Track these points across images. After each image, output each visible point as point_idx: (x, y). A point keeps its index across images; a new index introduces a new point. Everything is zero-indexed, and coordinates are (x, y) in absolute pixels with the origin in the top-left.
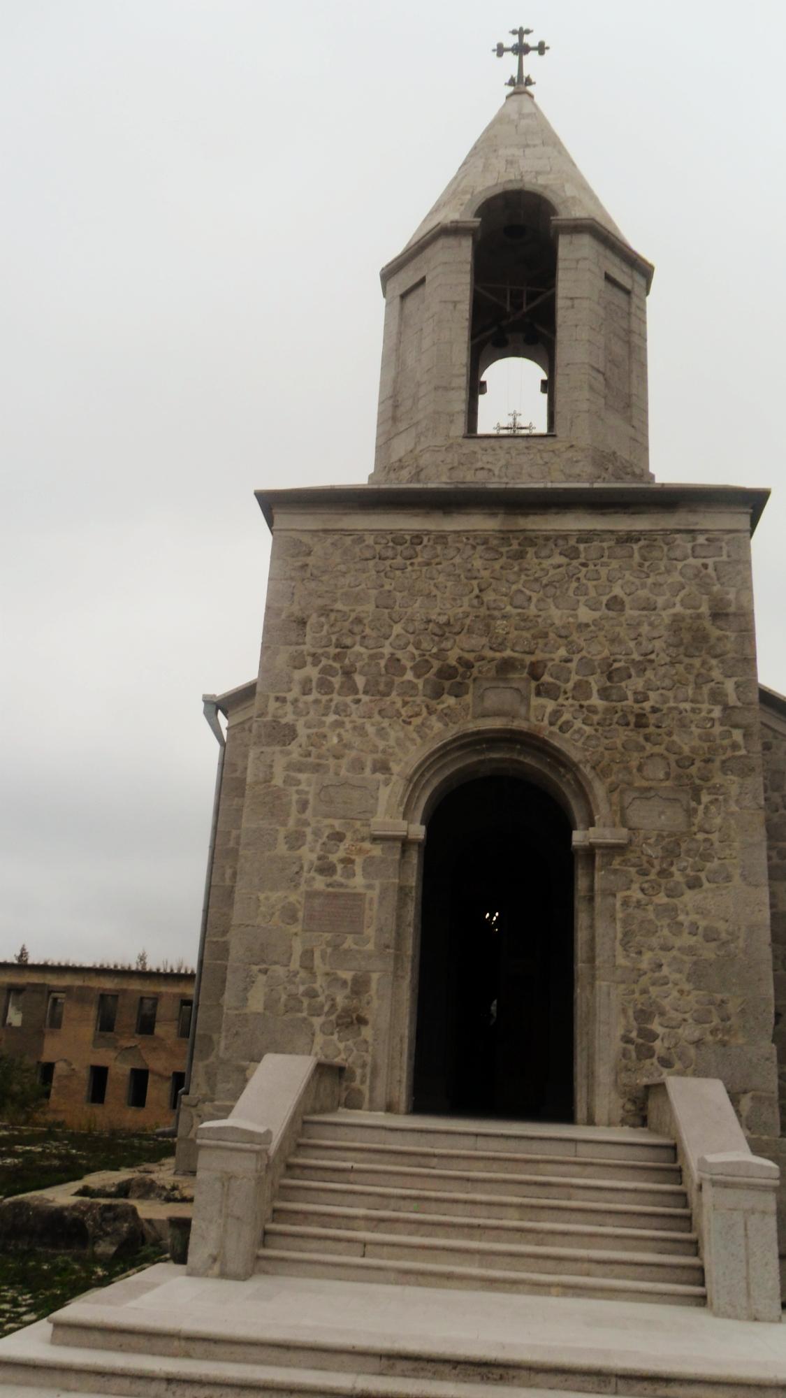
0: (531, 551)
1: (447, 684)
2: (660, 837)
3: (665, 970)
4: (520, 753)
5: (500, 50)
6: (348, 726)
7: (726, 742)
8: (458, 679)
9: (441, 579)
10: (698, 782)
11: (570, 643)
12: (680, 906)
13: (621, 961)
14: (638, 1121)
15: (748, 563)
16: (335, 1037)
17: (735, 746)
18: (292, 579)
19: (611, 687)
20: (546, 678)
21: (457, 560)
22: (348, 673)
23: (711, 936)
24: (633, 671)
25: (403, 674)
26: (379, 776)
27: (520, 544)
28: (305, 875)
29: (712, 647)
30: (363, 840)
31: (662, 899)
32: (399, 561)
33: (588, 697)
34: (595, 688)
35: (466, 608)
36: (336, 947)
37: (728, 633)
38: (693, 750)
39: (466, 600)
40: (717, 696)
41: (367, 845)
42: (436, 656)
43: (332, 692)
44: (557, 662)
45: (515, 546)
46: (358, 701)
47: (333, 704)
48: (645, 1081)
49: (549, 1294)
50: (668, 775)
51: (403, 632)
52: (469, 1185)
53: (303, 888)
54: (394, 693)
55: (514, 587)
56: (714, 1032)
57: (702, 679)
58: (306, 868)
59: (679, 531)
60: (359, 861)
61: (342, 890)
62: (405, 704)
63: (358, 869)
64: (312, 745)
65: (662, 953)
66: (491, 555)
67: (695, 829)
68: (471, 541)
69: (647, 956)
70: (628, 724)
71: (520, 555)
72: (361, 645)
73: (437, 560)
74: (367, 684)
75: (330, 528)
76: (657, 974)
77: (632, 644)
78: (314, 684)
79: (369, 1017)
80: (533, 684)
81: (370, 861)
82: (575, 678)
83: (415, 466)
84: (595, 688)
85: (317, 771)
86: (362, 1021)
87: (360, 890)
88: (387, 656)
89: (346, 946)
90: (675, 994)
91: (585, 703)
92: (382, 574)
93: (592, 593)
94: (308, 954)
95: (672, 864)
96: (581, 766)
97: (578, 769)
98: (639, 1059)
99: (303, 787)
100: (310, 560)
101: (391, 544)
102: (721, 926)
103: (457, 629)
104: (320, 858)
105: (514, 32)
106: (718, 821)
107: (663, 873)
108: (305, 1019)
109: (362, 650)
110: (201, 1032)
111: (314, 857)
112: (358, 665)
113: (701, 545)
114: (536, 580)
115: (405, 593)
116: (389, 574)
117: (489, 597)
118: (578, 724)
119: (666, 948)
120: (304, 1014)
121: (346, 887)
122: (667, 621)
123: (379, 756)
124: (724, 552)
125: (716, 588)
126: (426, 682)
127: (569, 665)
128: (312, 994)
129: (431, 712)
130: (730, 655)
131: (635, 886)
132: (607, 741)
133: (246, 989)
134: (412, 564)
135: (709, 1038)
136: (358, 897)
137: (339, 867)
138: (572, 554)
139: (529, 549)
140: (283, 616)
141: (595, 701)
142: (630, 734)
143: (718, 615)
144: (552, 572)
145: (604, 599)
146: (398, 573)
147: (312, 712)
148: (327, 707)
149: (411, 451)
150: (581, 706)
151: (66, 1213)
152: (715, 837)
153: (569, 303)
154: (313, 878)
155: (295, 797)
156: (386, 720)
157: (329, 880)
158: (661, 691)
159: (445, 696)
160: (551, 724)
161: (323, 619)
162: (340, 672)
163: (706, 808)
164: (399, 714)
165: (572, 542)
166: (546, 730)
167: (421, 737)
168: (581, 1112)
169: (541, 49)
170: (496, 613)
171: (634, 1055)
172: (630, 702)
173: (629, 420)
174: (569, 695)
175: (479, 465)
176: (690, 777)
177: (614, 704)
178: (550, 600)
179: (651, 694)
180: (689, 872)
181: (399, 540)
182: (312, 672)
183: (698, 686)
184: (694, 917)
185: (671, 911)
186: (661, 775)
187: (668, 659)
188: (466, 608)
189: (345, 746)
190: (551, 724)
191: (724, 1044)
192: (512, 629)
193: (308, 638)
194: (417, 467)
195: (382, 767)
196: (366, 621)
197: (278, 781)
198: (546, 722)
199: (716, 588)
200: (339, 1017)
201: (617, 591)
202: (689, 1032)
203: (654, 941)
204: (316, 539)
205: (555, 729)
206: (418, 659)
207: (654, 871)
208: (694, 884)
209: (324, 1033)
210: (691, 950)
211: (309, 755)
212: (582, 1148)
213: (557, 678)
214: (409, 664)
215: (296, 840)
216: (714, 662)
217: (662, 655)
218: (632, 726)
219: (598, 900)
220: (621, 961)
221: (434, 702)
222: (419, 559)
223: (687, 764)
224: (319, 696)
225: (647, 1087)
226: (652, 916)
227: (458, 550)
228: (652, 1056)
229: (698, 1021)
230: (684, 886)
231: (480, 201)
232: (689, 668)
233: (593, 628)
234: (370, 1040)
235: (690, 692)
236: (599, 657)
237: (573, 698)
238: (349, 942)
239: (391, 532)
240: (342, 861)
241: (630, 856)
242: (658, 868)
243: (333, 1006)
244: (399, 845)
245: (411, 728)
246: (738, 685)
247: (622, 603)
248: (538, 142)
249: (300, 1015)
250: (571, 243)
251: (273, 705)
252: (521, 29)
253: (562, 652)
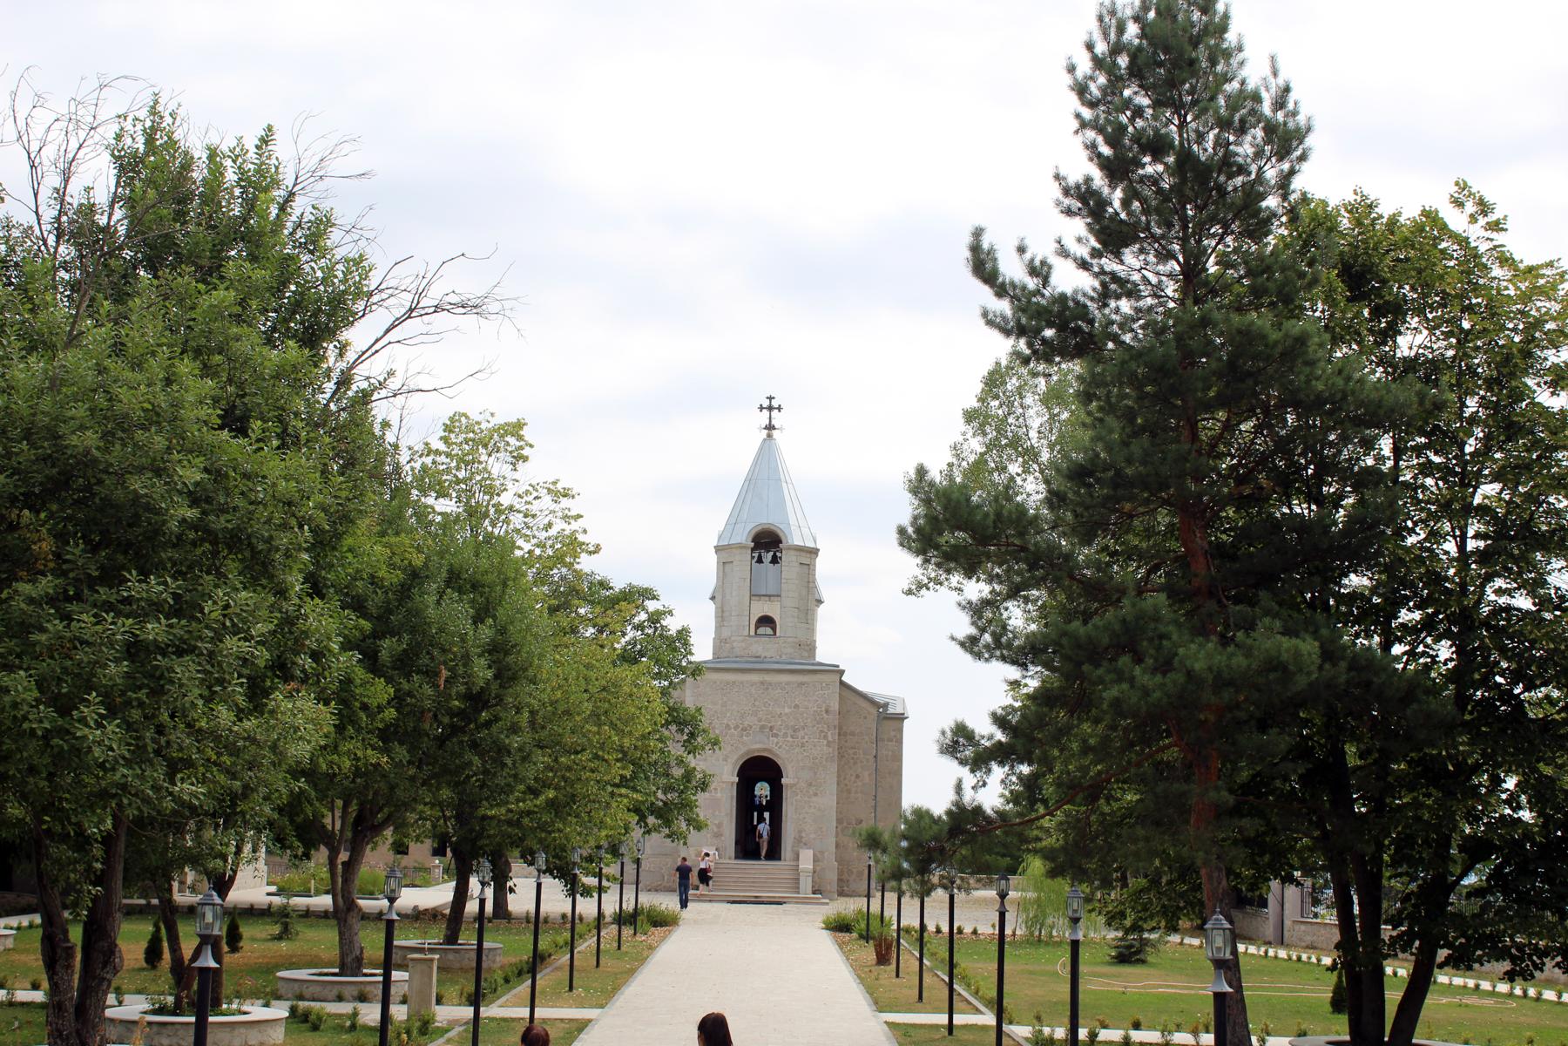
5: (761, 408)
141: (789, 739)
143: (827, 712)
166: (775, 749)
169: (779, 408)
181: (728, 683)
202: (812, 836)
208: (816, 795)
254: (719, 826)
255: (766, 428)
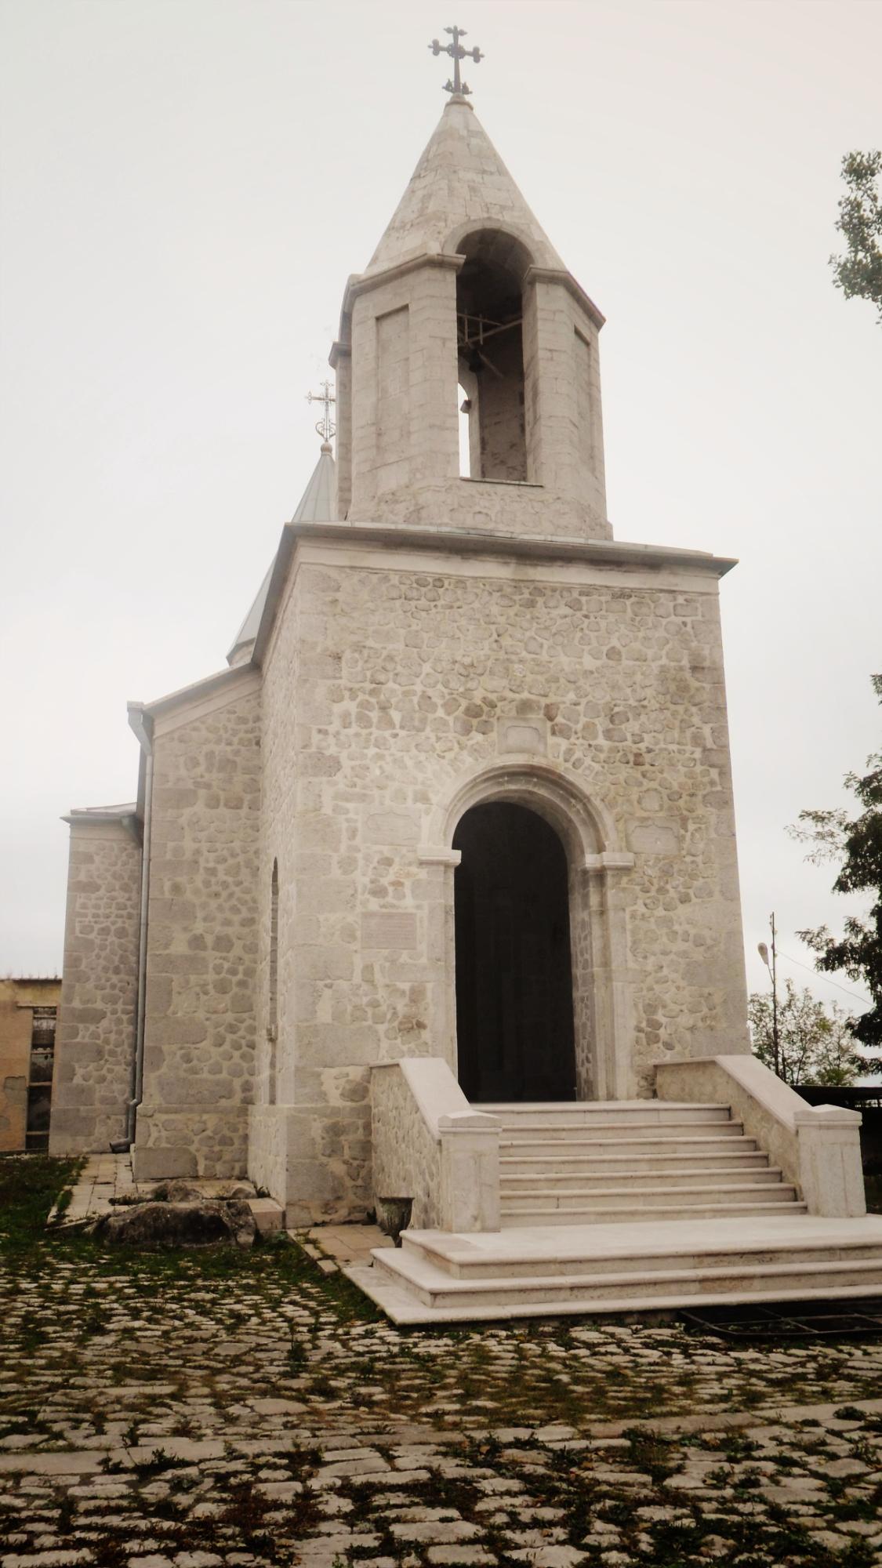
0: (540, 600)
1: (475, 722)
2: (658, 860)
3: (665, 971)
4: (535, 785)
5: (436, 48)
6: (389, 759)
7: (706, 780)
8: (484, 717)
9: (463, 622)
10: (685, 813)
11: (578, 688)
12: (675, 918)
13: (631, 965)
14: (650, 1094)
15: (717, 622)
16: (399, 1040)
17: (712, 783)
18: (324, 613)
19: (614, 729)
20: (559, 719)
21: (476, 605)
22: (384, 708)
23: (699, 942)
24: (630, 715)
25: (435, 711)
26: (419, 805)
27: (530, 594)
28: (359, 897)
29: (692, 697)
30: (410, 864)
31: (660, 912)
32: (423, 602)
33: (595, 738)
34: (600, 729)
35: (487, 651)
36: (393, 962)
37: (704, 685)
38: (681, 785)
39: (486, 644)
40: (697, 740)
41: (414, 869)
42: (462, 695)
43: (371, 726)
44: (568, 704)
45: (526, 596)
46: (395, 736)
47: (372, 738)
48: (657, 1062)
49: (704, 1218)
50: (661, 806)
51: (432, 671)
52: (601, 1149)
53: (359, 909)
54: (428, 729)
55: (528, 634)
56: (704, 1019)
57: (685, 725)
58: (360, 890)
59: (662, 591)
60: (408, 883)
61: (394, 911)
62: (439, 739)
63: (407, 890)
64: (357, 776)
65: (662, 957)
66: (506, 602)
67: (684, 852)
68: (487, 587)
69: (651, 960)
70: (628, 763)
71: (531, 604)
72: (395, 682)
73: (458, 604)
74: (403, 718)
75: (357, 565)
76: (659, 975)
77: (629, 691)
78: (353, 718)
79: (426, 1022)
80: (549, 724)
81: (417, 885)
82: (583, 720)
83: (413, 502)
84: (600, 729)
85: (364, 801)
86: (421, 1026)
87: (414, 911)
88: (419, 693)
89: (402, 960)
90: (674, 989)
91: (593, 743)
92: (409, 614)
93: (594, 643)
94: (368, 968)
95: (667, 882)
96: (592, 798)
97: (589, 800)
98: (648, 1044)
99: (351, 815)
100: (339, 596)
101: (415, 585)
102: (706, 933)
103: (480, 671)
104: (372, 882)
105: (449, 31)
106: (701, 846)
107: (661, 890)
108: (370, 1027)
109: (396, 687)
110: (151, 1044)
111: (366, 880)
112: (393, 701)
113: (681, 605)
114: (546, 628)
115: (431, 634)
116: (415, 614)
117: (506, 641)
118: (588, 761)
119: (665, 953)
120: (370, 1022)
121: (398, 907)
122: (656, 671)
123: (419, 787)
124: (700, 613)
125: (694, 644)
126: (456, 719)
127: (578, 707)
128: (375, 1004)
129: (462, 748)
130: (707, 704)
131: (640, 902)
132: (612, 777)
133: (314, 1003)
134: (435, 606)
135: (700, 1024)
136: (411, 916)
137: (391, 889)
138: (575, 606)
139: (538, 598)
140: (319, 650)
141: (601, 741)
142: (631, 771)
143: (695, 669)
144: (559, 622)
145: (605, 649)
146: (424, 614)
147: (353, 745)
148: (367, 741)
149: (407, 487)
150: (590, 745)
151: (202, 1213)
152: (699, 859)
153: (549, 354)
154: (368, 900)
155: (345, 825)
156: (423, 754)
157: (382, 901)
158: (653, 734)
159: (474, 733)
160: (566, 761)
161: (357, 655)
162: (377, 706)
163: (692, 834)
164: (434, 749)
165: (575, 594)
166: (562, 768)
167: (455, 771)
168: (602, 1091)
170: (513, 657)
171: (644, 1041)
172: (629, 743)
173: (593, 470)
174: (580, 735)
175: (478, 509)
176: (679, 809)
177: (617, 744)
178: (559, 648)
179: (645, 735)
180: (681, 888)
181: (421, 583)
182: (351, 706)
183: (682, 731)
184: (687, 927)
185: (667, 922)
186: (657, 808)
187: (658, 706)
188: (487, 651)
189: (387, 777)
190: (566, 761)
191: (712, 1028)
192: (528, 674)
193: (344, 673)
194: (417, 504)
195: (423, 798)
196: (397, 659)
197: (327, 810)
198: (561, 759)
199: (694, 644)
200: (401, 1023)
201: (615, 642)
202: (686, 1020)
203: (657, 947)
204: (344, 575)
205: (569, 765)
206: (447, 697)
207: (654, 889)
208: (685, 900)
209: (388, 1038)
210: (684, 954)
211: (355, 785)
212: (663, 1115)
213: (569, 720)
214: (440, 702)
215: (348, 865)
216: (694, 709)
217: (653, 701)
218: (632, 764)
219: (612, 915)
220: (631, 965)
221: (463, 739)
222: (440, 603)
223: (676, 797)
224: (359, 730)
225: (656, 1067)
226: (653, 927)
227: (477, 595)
228: (658, 1042)
229: (691, 1012)
230: (678, 903)
231: (461, 234)
232: (674, 714)
233: (596, 675)
234: (430, 1043)
235: (676, 735)
236: (603, 701)
237: (583, 738)
238: (404, 957)
239: (415, 573)
240: (393, 884)
241: (634, 876)
242: (656, 886)
243: (395, 1014)
244: (442, 868)
245: (445, 762)
246: (713, 730)
247: (619, 653)
248: (493, 169)
249: (365, 1023)
250: (548, 293)
251: (316, 738)
252: (456, 28)
253: (571, 696)
254: (416, 996)
255: (448, 87)
